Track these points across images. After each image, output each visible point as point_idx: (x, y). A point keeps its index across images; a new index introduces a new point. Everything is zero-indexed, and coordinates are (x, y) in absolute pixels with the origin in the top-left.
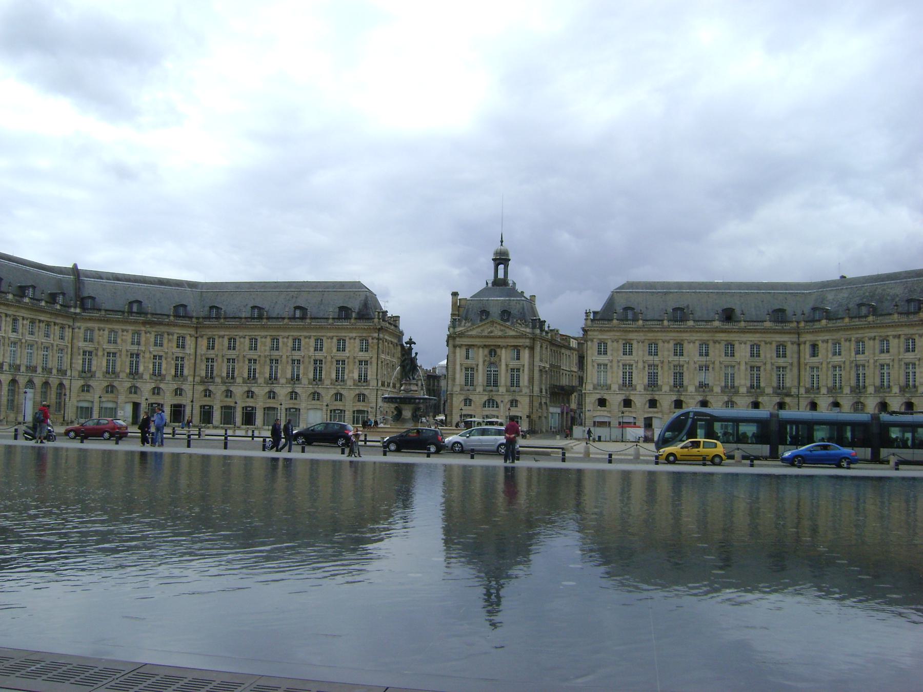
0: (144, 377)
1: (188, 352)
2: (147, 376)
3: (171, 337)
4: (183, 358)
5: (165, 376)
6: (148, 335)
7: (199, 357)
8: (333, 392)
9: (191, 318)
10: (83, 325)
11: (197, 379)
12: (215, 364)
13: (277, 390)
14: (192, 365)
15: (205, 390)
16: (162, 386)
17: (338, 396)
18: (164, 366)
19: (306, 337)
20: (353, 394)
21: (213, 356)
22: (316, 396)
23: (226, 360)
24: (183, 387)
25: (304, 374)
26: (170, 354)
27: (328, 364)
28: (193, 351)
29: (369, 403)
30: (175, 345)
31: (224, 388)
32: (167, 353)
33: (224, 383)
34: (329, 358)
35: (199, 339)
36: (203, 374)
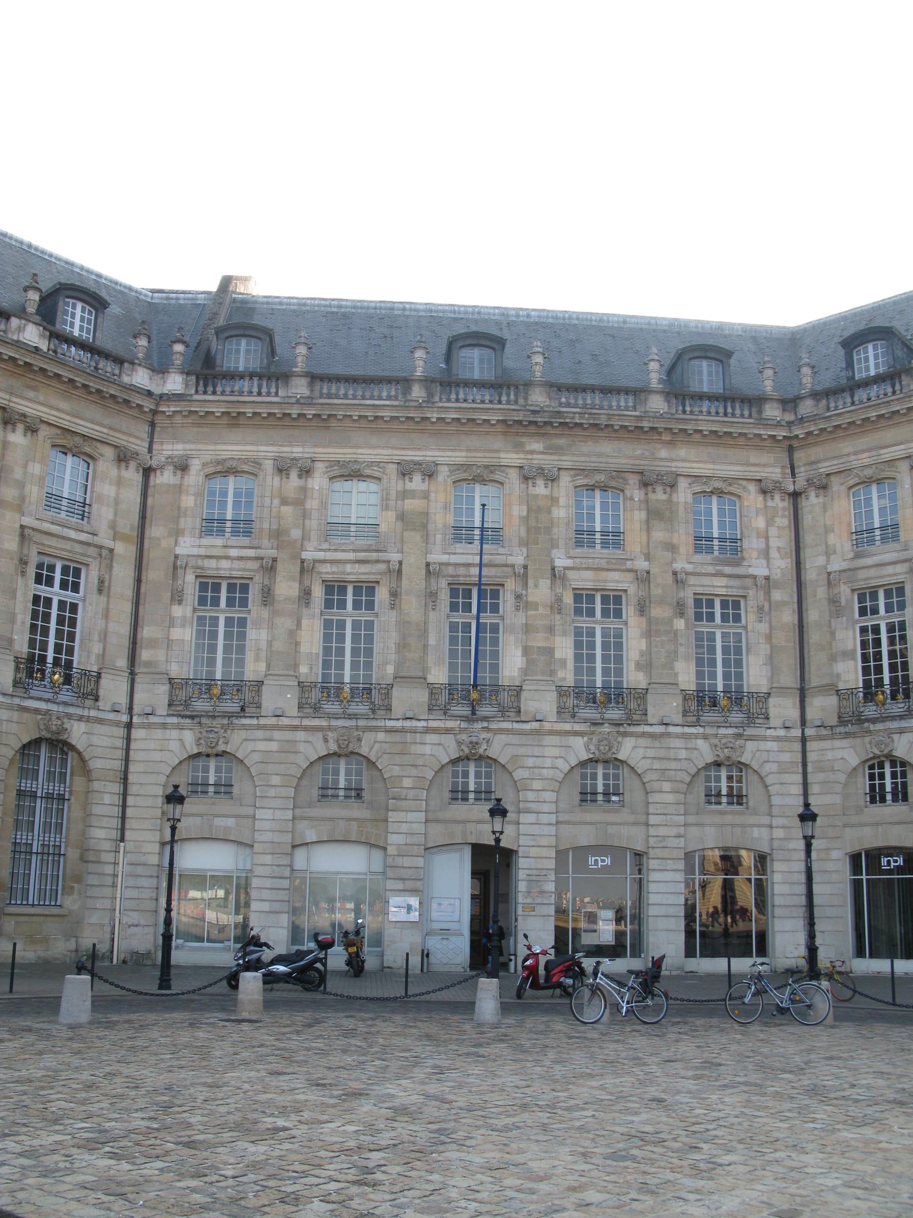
0: (531, 703)
1: (759, 569)
2: (541, 702)
3: (659, 495)
4: (732, 608)
5: (641, 695)
6: (540, 488)
7: (817, 594)
9: (755, 402)
10: (204, 451)
11: (822, 707)
14: (786, 640)
15: (874, 767)
16: (629, 749)
18: (634, 644)
24: (749, 753)
26: (662, 580)
28: (782, 565)
30: (683, 537)
32: (644, 578)
35: (812, 502)
36: (851, 674)
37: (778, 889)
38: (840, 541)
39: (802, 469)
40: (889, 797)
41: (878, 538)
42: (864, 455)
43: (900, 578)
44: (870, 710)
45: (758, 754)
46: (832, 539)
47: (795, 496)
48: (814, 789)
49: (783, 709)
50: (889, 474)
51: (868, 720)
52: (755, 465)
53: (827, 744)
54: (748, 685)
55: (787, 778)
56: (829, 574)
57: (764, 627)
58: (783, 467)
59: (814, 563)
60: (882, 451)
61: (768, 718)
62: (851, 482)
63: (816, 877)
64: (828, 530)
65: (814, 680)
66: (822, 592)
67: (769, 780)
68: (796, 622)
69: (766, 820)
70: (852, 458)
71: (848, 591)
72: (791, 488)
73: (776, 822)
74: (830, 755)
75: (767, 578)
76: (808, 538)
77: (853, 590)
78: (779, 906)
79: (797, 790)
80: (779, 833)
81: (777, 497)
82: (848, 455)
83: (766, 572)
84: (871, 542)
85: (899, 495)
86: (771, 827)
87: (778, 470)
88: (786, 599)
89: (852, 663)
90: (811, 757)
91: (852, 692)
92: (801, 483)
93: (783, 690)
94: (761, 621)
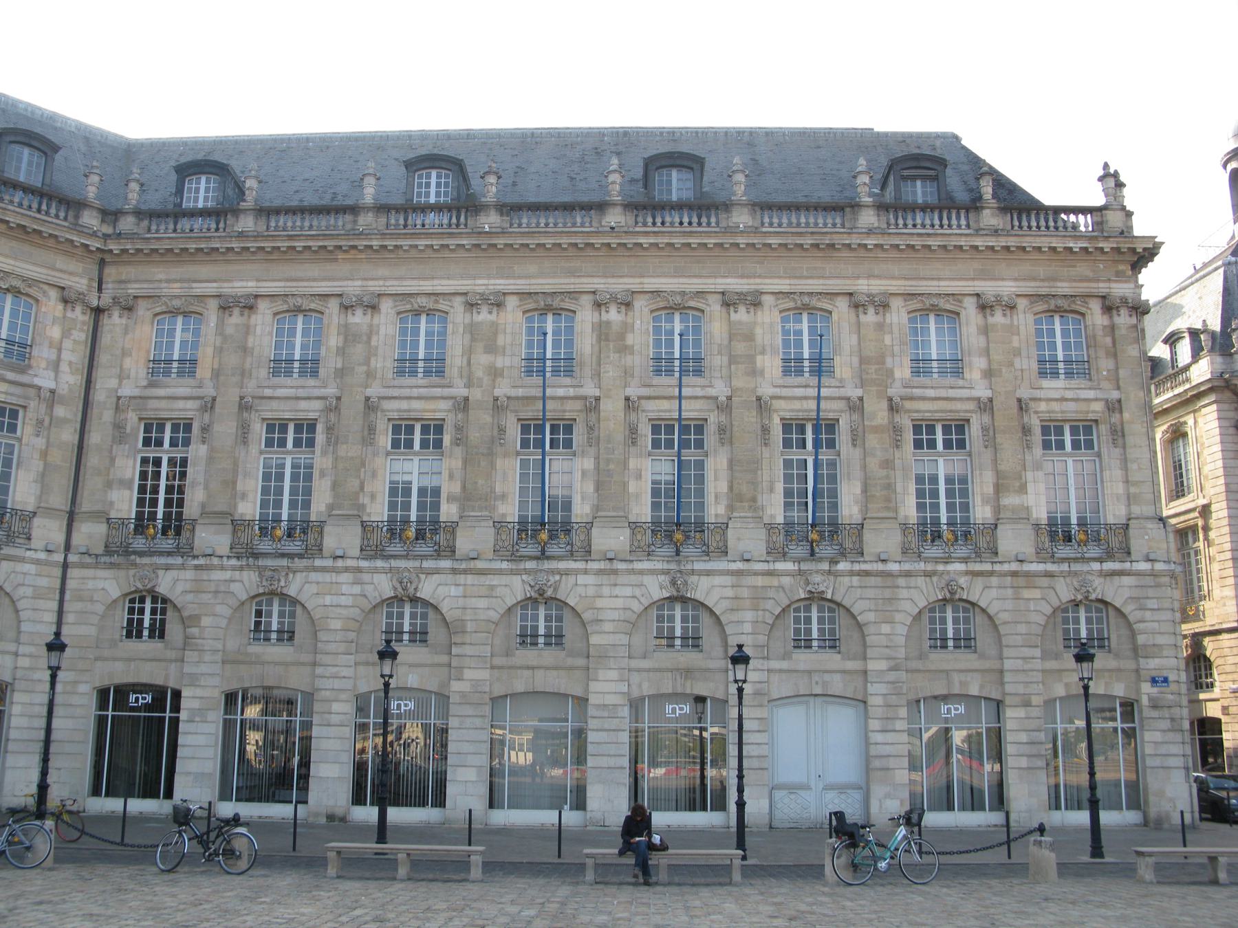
1: (45, 380)
7: (103, 416)
8: (918, 595)
9: (73, 205)
11: (90, 533)
12: (197, 452)
13: (579, 585)
14: (63, 459)
15: (135, 601)
17: (954, 624)
19: (729, 302)
20: (1039, 604)
21: (186, 409)
22: (821, 624)
23: (259, 430)
25: (735, 498)
27: (872, 441)
28: (70, 380)
29: (1136, 651)
31: (246, 582)
33: (246, 553)
34: (878, 412)
35: (114, 322)
36: (125, 504)
37: (15, 722)
38: (137, 367)
39: (110, 286)
40: (146, 633)
41: (175, 370)
42: (178, 285)
43: (189, 414)
44: (139, 543)
45: (13, 575)
46: (128, 362)
47: (98, 311)
48: (69, 618)
49: (48, 531)
50: (199, 309)
51: (135, 553)
52: (61, 271)
53: (90, 573)
54: (13, 501)
55: (41, 604)
56: (119, 398)
57: (40, 442)
58: (91, 279)
59: (105, 384)
60: (194, 285)
61: (29, 539)
62: (158, 310)
63: (57, 711)
64: (125, 353)
65: (85, 505)
66: (108, 416)
67: (21, 605)
68: (76, 442)
69: (12, 647)
70: (164, 285)
71: (136, 419)
72: (95, 303)
73: (23, 649)
74: (90, 584)
75: (53, 392)
76: (103, 358)
77: (141, 419)
78: (15, 740)
79: (51, 617)
80: (24, 662)
81: (78, 309)
82: (160, 281)
83: (52, 385)
84: (167, 373)
85: (203, 332)
86: (16, 654)
87: (85, 281)
88: (69, 416)
89: (127, 493)
90: (71, 584)
91: (123, 522)
92: (106, 299)
93: (50, 512)
94: (38, 436)
